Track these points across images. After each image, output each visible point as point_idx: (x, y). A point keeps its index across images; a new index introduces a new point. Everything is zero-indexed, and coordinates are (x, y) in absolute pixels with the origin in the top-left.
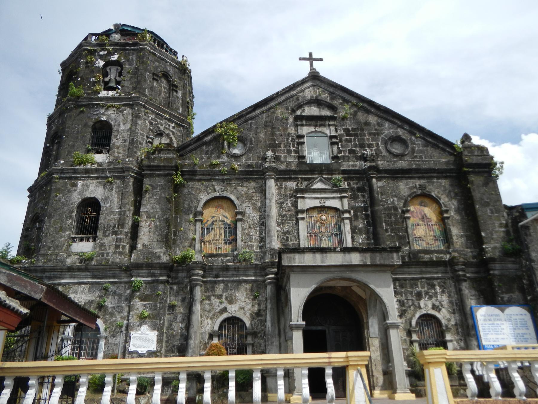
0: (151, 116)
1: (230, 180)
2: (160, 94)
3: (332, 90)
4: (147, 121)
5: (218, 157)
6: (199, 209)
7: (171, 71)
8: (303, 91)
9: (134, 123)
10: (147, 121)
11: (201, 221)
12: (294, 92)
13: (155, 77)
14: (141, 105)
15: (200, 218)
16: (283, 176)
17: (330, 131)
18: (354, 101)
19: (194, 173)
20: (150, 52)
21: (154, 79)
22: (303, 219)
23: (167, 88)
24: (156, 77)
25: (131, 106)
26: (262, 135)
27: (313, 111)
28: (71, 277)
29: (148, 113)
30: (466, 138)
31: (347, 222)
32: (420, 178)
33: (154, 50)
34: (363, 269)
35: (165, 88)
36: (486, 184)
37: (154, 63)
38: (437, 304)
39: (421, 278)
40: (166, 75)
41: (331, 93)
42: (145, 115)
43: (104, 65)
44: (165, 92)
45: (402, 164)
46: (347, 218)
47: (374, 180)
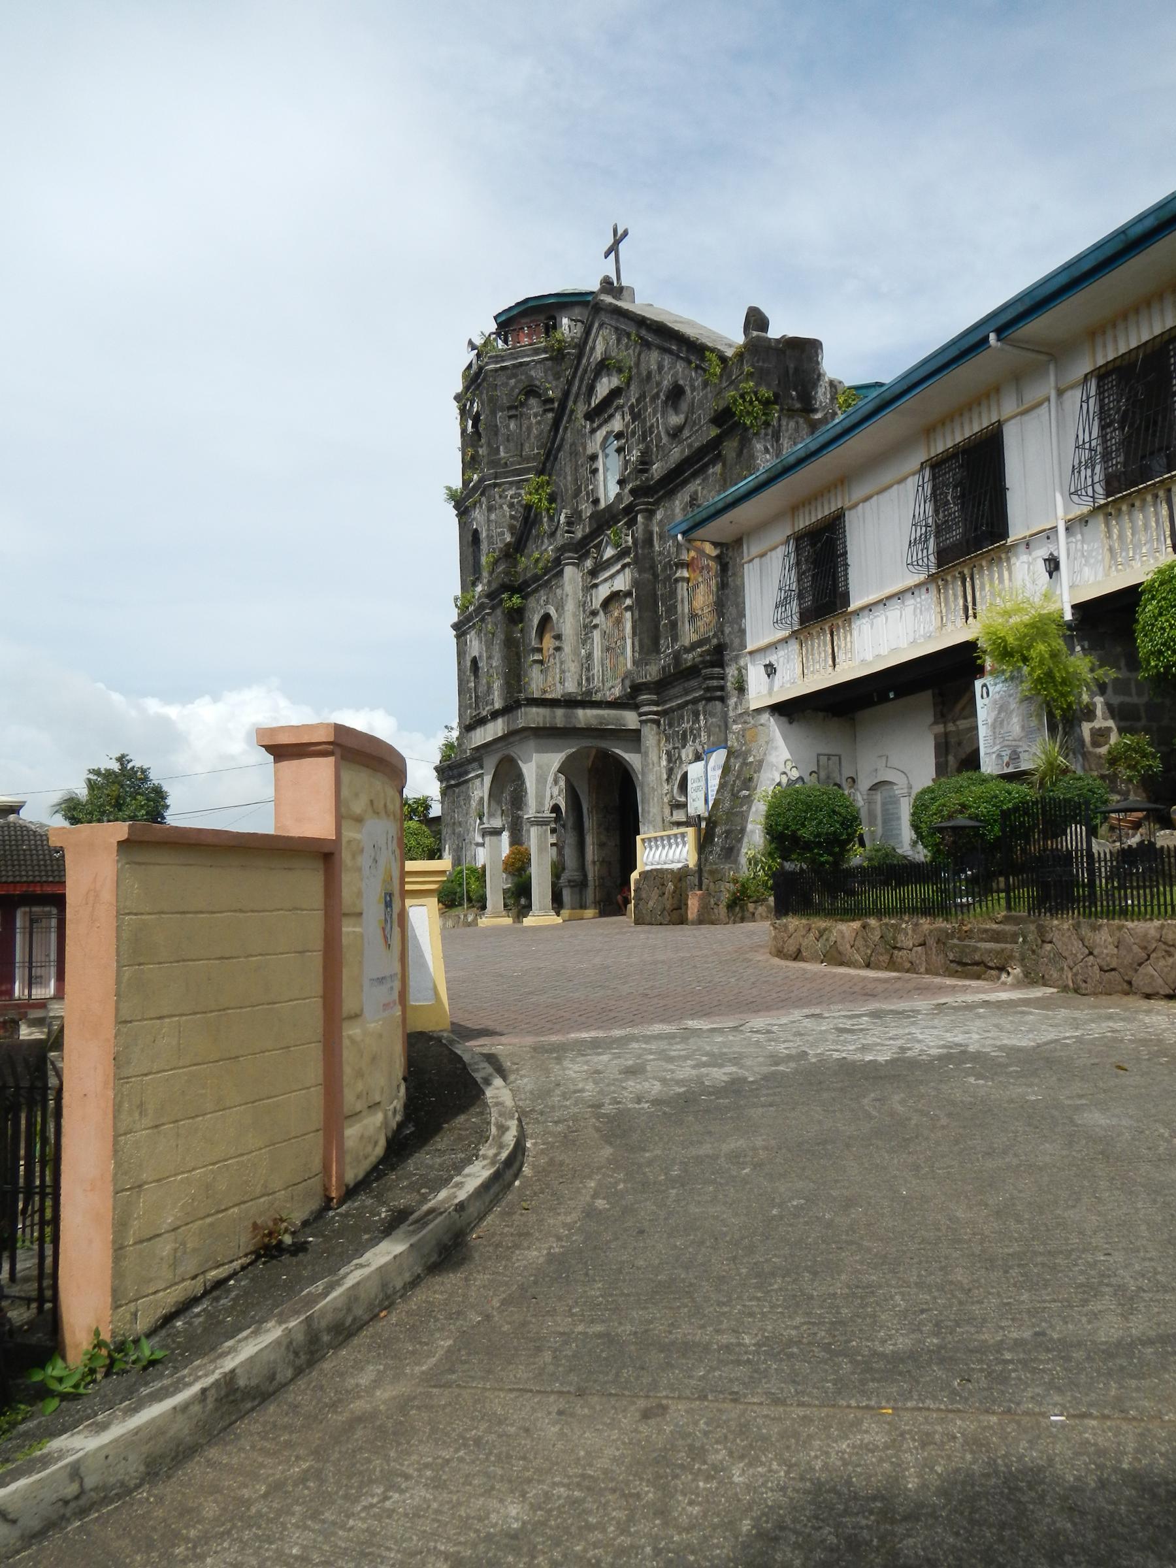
0: (510, 493)
1: (549, 580)
2: (529, 435)
3: (613, 323)
4: (505, 507)
5: (542, 542)
6: (534, 643)
7: (537, 374)
8: (593, 349)
9: (489, 521)
10: (505, 507)
11: (541, 662)
12: (584, 361)
13: (511, 413)
14: (489, 485)
15: (537, 657)
16: (581, 549)
17: (617, 424)
18: (633, 330)
19: (526, 584)
20: (496, 370)
21: (510, 417)
22: (596, 626)
23: (541, 410)
24: (515, 409)
25: (482, 494)
26: (569, 478)
27: (604, 387)
28: (474, 770)
29: (504, 491)
30: (756, 320)
31: (628, 615)
32: (694, 475)
33: (503, 361)
34: (517, 738)
35: (536, 415)
36: (740, 453)
37: (506, 384)
38: (700, 750)
39: (687, 703)
40: (531, 391)
41: (617, 329)
42: (500, 497)
43: (475, 425)
44: (539, 423)
45: (677, 454)
46: (628, 608)
47: (640, 518)
